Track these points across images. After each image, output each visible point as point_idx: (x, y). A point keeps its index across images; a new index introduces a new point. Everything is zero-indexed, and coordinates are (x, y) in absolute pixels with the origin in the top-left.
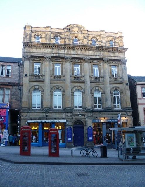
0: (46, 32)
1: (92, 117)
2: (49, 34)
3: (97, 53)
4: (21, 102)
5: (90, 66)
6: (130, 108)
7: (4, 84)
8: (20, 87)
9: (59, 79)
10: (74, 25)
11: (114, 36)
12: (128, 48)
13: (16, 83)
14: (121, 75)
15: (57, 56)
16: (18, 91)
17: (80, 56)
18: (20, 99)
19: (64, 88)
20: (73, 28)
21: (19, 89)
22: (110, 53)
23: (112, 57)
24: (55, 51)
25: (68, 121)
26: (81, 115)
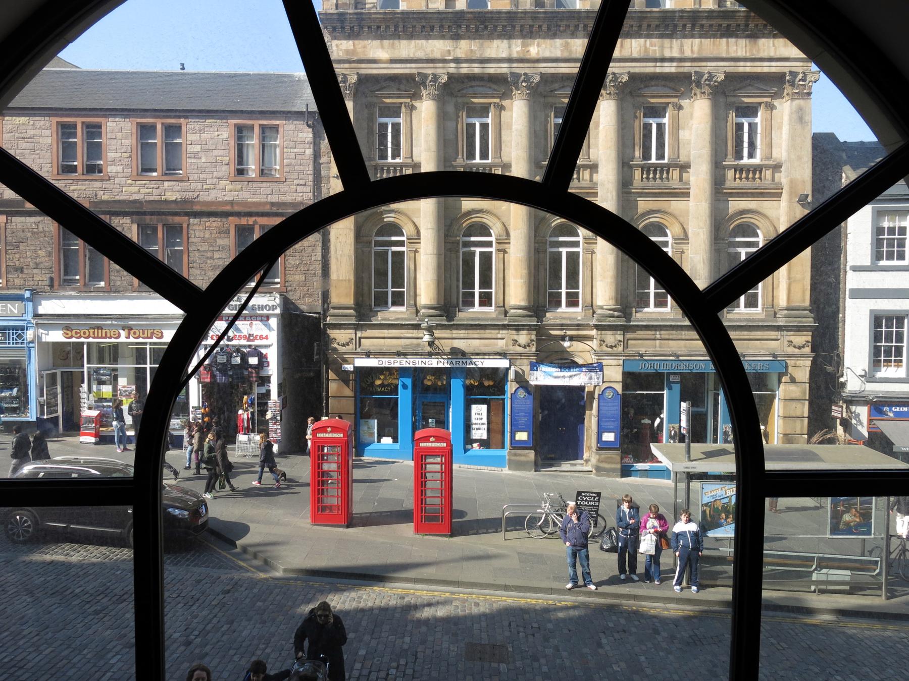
1: (621, 348)
3: (667, 42)
7: (254, 210)
15: (477, 71)
22: (732, 41)
23: (742, 64)
24: (464, 48)
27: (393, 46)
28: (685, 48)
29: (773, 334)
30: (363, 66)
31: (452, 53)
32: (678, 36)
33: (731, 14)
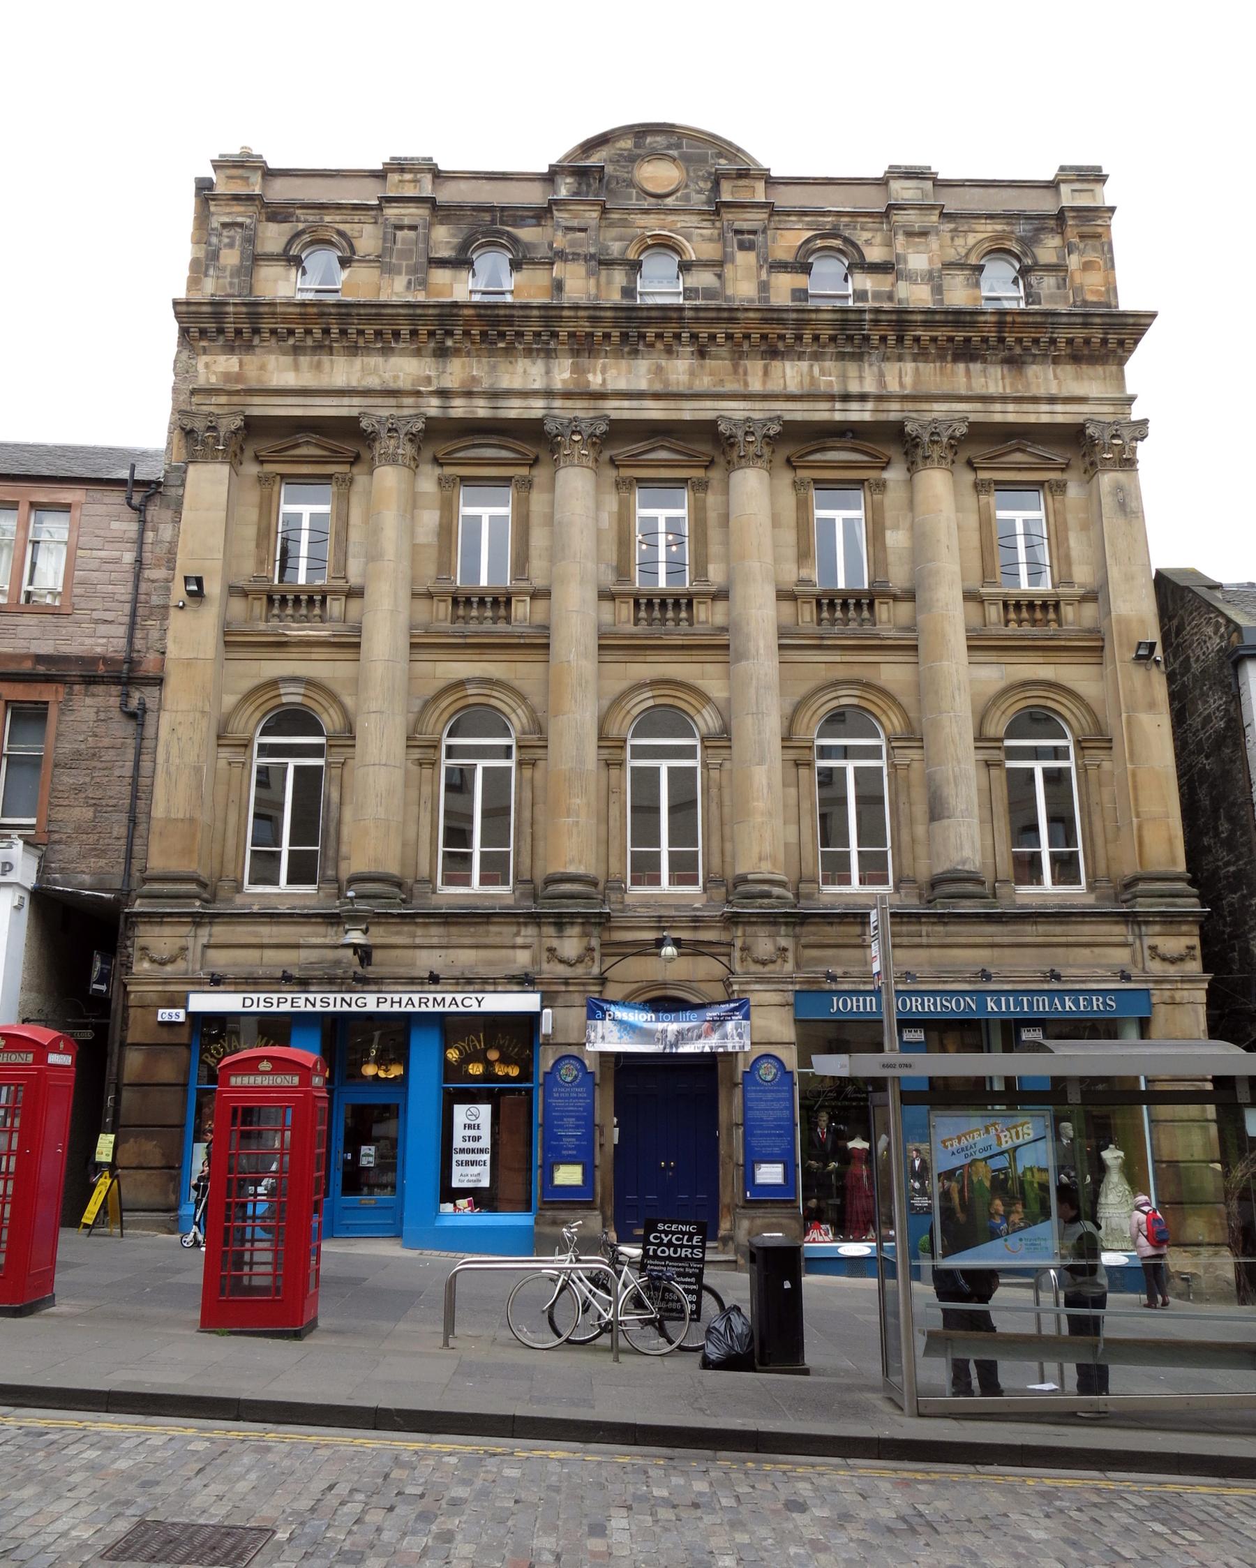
0: (391, 212)
1: (789, 967)
2: (413, 228)
3: (852, 368)
4: (142, 828)
5: (788, 500)
6: (1181, 886)
8: (136, 696)
9: (495, 620)
10: (641, 132)
11: (1010, 217)
12: (1153, 316)
13: (105, 660)
14: (1082, 575)
15: (482, 413)
16: (122, 729)
17: (688, 412)
18: (135, 797)
19: (536, 700)
20: (632, 159)
21: (132, 716)
22: (976, 367)
23: (998, 407)
24: (455, 372)
25: (560, 1001)
26: (677, 943)
27: (318, 366)
28: (888, 379)
29: (1118, 931)
30: (257, 400)
31: (435, 382)
32: (873, 358)
33: (968, 318)
